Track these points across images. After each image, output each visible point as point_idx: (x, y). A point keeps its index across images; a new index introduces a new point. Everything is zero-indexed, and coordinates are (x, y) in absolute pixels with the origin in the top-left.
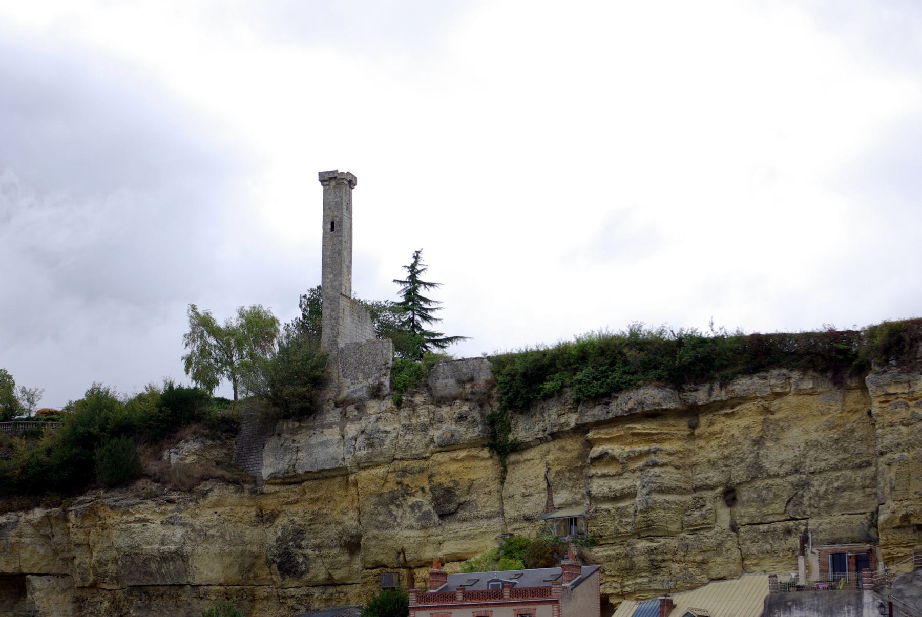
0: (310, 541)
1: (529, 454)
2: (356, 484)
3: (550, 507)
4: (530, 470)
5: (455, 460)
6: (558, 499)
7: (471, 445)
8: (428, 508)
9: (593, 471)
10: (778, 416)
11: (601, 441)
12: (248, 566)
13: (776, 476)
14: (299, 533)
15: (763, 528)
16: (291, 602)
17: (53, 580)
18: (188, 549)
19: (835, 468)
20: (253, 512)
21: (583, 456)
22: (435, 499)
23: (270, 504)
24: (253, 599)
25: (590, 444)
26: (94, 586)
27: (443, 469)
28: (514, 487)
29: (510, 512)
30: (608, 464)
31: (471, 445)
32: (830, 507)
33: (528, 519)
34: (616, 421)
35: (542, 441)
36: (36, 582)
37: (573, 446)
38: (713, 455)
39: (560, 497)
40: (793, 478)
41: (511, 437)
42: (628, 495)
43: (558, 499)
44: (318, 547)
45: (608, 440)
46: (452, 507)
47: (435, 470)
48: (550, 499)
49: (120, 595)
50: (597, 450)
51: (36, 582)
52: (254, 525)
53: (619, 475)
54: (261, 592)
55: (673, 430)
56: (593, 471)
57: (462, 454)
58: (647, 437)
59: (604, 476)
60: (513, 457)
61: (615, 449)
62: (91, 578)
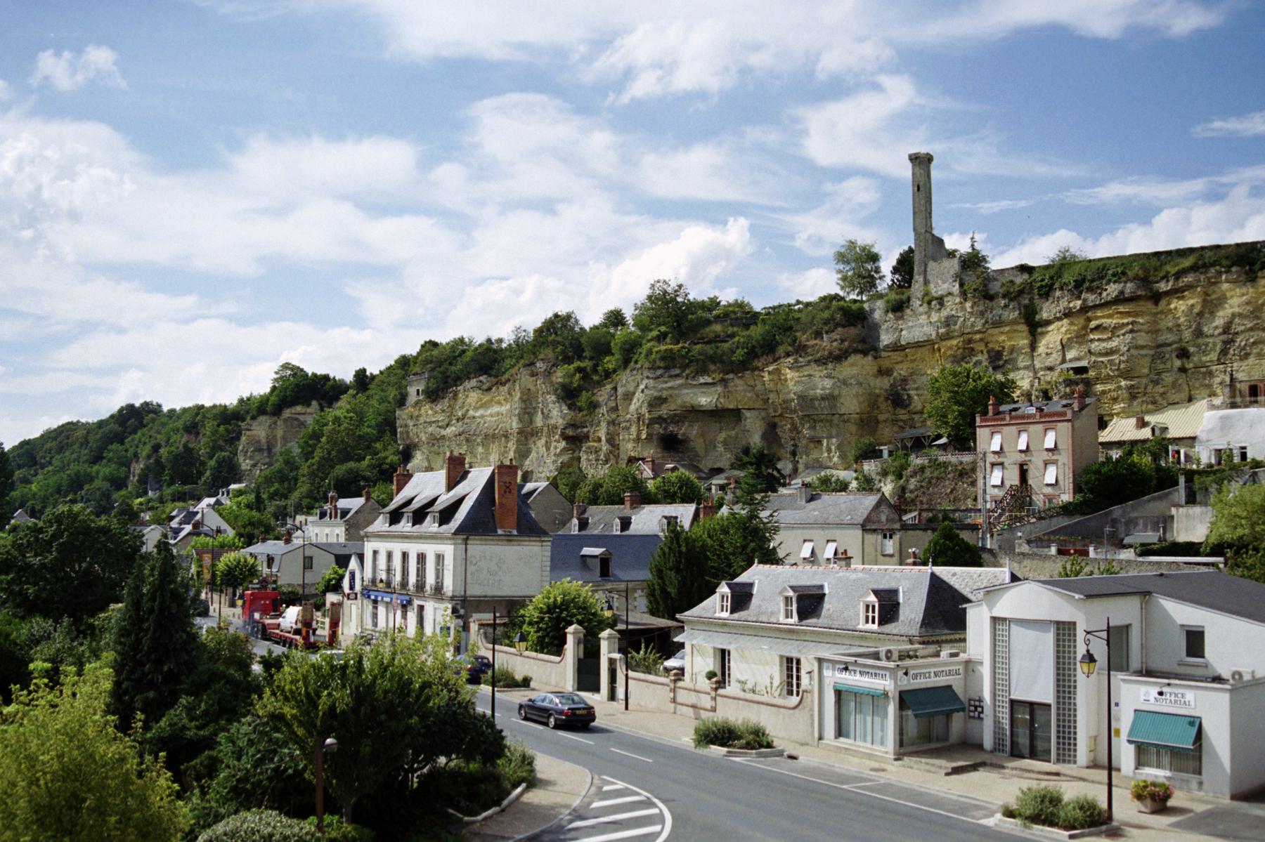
0: (911, 385)
1: (1050, 328)
2: (939, 350)
3: (1064, 361)
4: (1054, 336)
5: (1002, 333)
6: (1069, 355)
7: (1014, 322)
8: (985, 363)
9: (1092, 336)
10: (1213, 297)
11: (1097, 318)
12: (873, 402)
13: (1212, 336)
14: (904, 380)
15: (1203, 370)
16: (901, 424)
17: (756, 413)
18: (836, 392)
19: (1251, 329)
20: (875, 369)
21: (1085, 327)
22: (990, 357)
23: (886, 364)
24: (877, 422)
25: (1089, 320)
26: (781, 415)
27: (994, 339)
28: (1041, 349)
29: (1038, 365)
30: (1102, 333)
31: (1014, 322)
32: (1247, 356)
33: (1051, 369)
34: (1107, 304)
35: (1059, 319)
36: (748, 414)
37: (1080, 321)
38: (1170, 324)
39: (1070, 355)
40: (1224, 337)
41: (1037, 317)
42: (1111, 352)
43: (1069, 355)
44: (916, 389)
45: (1103, 317)
46: (1001, 363)
47: (990, 339)
48: (1064, 355)
49: (797, 421)
50: (1093, 324)
51: (748, 414)
52: (876, 376)
53: (1110, 339)
54: (882, 417)
55: (1143, 309)
56: (1092, 336)
57: (1007, 329)
58: (1128, 314)
59: (1099, 340)
60: (1039, 330)
61: (1106, 322)
62: (780, 411)
